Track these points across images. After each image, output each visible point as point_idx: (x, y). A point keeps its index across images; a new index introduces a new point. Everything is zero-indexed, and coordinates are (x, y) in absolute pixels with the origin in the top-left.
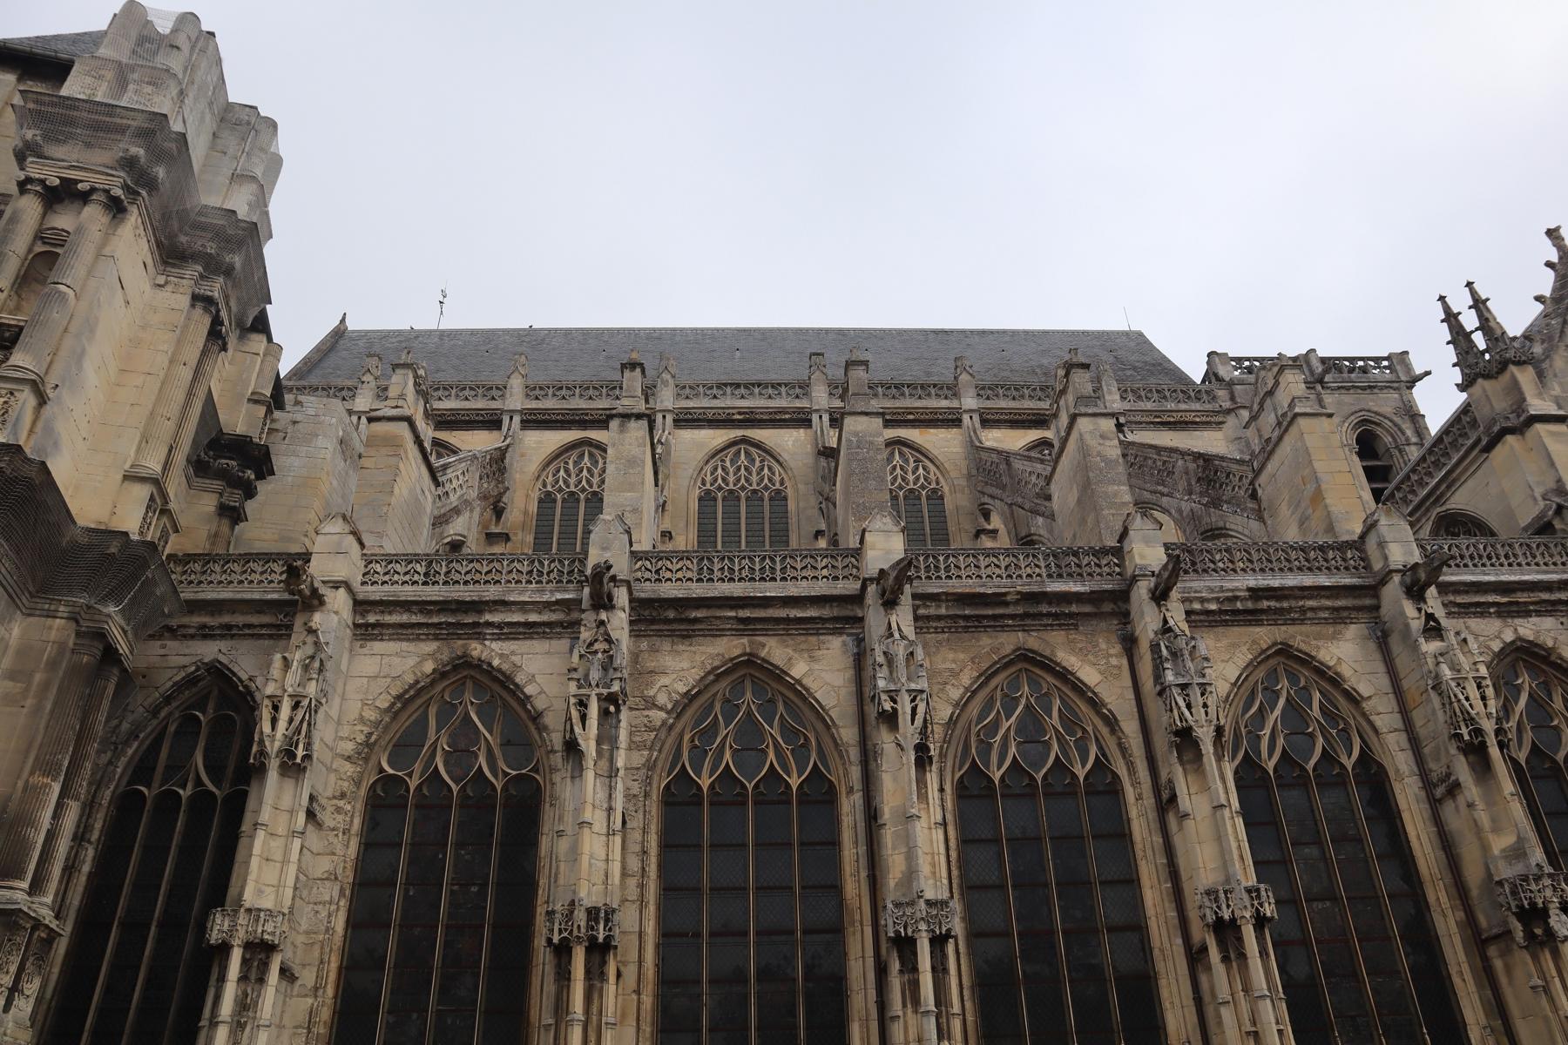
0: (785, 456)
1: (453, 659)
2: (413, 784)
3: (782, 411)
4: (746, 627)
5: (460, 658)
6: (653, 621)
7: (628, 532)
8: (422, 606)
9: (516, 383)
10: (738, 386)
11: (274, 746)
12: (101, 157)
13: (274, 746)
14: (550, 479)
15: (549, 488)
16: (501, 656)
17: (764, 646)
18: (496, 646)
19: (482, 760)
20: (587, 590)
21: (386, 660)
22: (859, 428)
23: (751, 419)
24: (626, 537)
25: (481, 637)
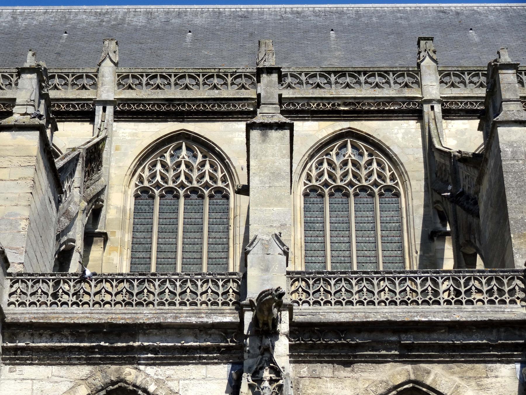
0: (395, 150)
1: (107, 385)
3: (391, 100)
4: (407, 354)
5: (113, 383)
6: (313, 347)
7: (286, 253)
8: (75, 330)
9: (108, 71)
10: (342, 74)
14: (146, 174)
15: (146, 184)
16: (157, 381)
17: (429, 373)
18: (151, 370)
20: (248, 317)
21: (37, 385)
22: (513, 138)
23: (358, 110)
24: (285, 258)
25: (133, 361)
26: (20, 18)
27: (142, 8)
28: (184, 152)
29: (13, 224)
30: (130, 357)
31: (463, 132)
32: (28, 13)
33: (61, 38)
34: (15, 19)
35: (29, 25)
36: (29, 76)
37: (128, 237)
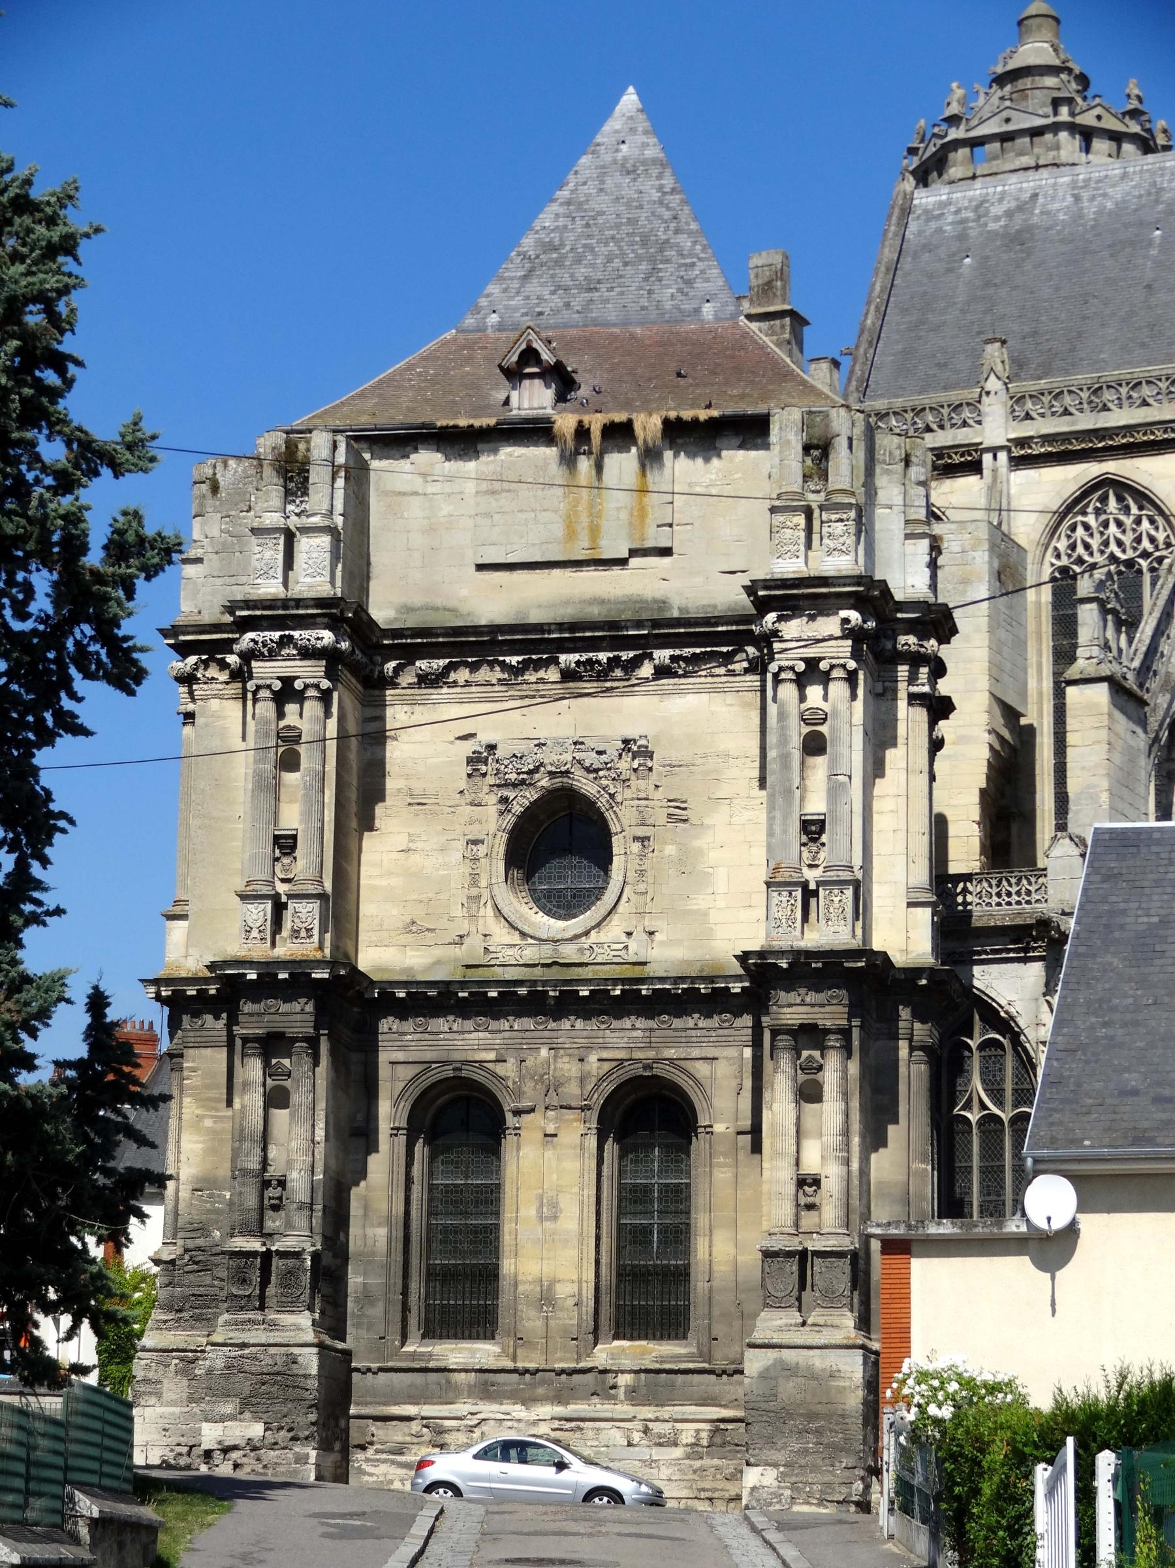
12: (829, 625)
26: (1085, 195)
29: (1094, 798)
32: (1099, 181)
33: (1150, 243)
34: (1077, 198)
35: (1100, 212)
36: (1088, 606)
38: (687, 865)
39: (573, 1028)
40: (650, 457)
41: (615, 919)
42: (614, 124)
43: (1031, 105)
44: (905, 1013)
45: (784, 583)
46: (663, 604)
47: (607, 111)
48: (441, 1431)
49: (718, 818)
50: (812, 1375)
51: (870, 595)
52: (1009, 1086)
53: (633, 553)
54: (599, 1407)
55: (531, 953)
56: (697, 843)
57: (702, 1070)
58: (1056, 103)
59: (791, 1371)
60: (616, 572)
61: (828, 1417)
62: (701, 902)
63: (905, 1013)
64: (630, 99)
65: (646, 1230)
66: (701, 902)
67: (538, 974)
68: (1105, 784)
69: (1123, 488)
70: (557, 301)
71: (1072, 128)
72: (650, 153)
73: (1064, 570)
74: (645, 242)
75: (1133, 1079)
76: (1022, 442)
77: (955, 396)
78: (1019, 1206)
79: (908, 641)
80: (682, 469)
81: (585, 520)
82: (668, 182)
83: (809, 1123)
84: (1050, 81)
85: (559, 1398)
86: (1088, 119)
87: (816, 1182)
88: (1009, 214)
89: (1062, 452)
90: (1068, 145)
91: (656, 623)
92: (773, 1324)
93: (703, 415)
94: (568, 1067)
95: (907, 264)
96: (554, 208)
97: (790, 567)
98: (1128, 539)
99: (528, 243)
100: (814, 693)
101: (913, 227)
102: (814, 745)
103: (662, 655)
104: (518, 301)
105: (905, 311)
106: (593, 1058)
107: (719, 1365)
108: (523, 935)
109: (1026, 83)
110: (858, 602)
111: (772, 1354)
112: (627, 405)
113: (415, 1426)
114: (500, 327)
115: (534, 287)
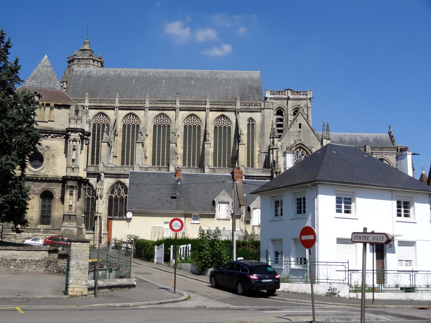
0: (170, 117)
2: (114, 197)
9: (117, 99)
11: (99, 195)
12: (77, 134)
13: (99, 195)
19: (122, 194)
23: (164, 109)
27: (124, 69)
28: (132, 117)
30: (120, 178)
31: (183, 114)
35: (100, 75)
37: (122, 134)
38: (54, 163)
39: (37, 183)
40: (52, 109)
41: (44, 170)
42: (44, 60)
43: (86, 54)
44: (82, 184)
45: (72, 128)
46: (52, 128)
47: (43, 58)
48: (16, 236)
49: (58, 157)
50: (70, 230)
51: (83, 131)
52: (91, 193)
53: (49, 121)
54: (38, 234)
55: (32, 173)
56: (56, 160)
57: (55, 190)
58: (90, 55)
59: (67, 230)
60: (46, 123)
61: (72, 236)
62: (56, 168)
63: (82, 184)
64: (46, 57)
65: (45, 211)
66: (56, 168)
67: (32, 176)
68: (106, 156)
69: (103, 114)
70: (36, 84)
71: (92, 59)
72: (49, 65)
73: (95, 124)
74: (49, 77)
75: (138, 202)
76: (90, 106)
77: (81, 98)
78: (126, 216)
79: (86, 137)
80: (56, 110)
81: (42, 116)
82: (52, 69)
83: (71, 198)
84: (88, 52)
85: (33, 233)
86: (94, 58)
87: (71, 206)
88: (87, 73)
89: (96, 108)
90: (91, 62)
91: (52, 131)
92: (65, 224)
93: (60, 104)
94: (36, 189)
95: (73, 78)
96: (35, 70)
97: (73, 126)
98: (103, 121)
99: (32, 75)
100: (74, 143)
101: (74, 73)
102: (74, 149)
103: (52, 135)
104: (31, 83)
105: (73, 85)
106: (40, 188)
107: (55, 229)
108: (31, 171)
109: (85, 51)
110: (81, 132)
111: (65, 228)
112: (48, 101)
113: (12, 236)
114: (28, 87)
115: (33, 81)
